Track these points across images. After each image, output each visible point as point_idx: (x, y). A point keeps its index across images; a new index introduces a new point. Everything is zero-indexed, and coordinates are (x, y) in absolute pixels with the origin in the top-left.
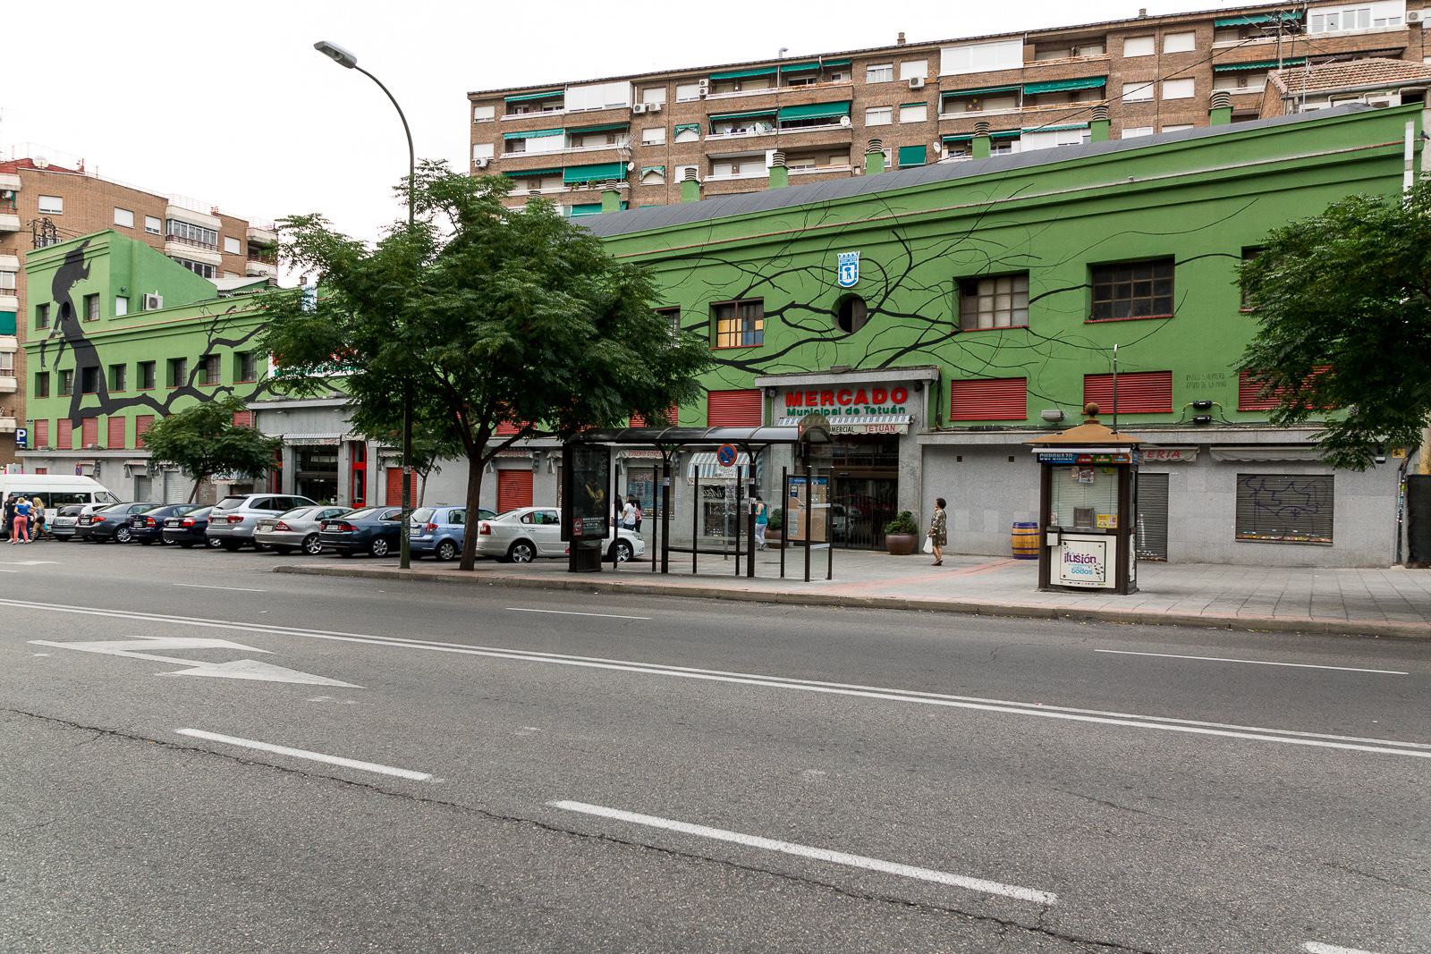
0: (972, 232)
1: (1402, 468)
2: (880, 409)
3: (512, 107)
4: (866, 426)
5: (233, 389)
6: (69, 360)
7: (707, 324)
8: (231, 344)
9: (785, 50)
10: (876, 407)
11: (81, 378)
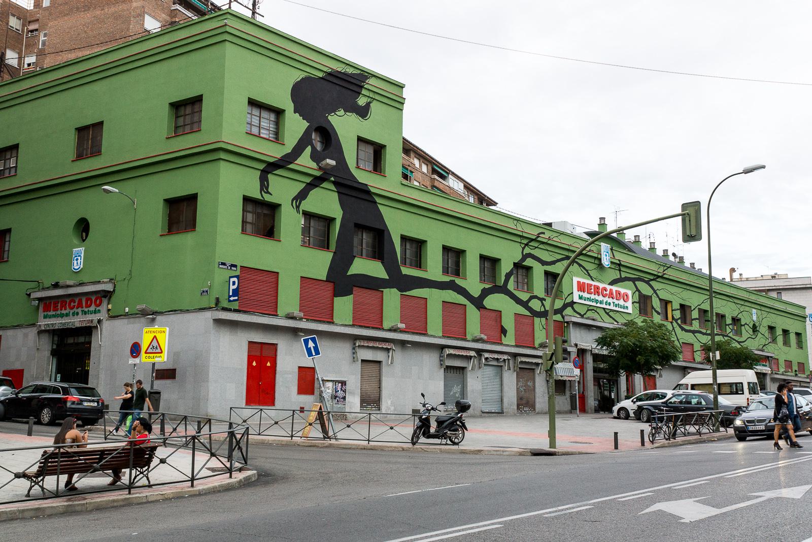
5: (545, 300)
8: (544, 263)
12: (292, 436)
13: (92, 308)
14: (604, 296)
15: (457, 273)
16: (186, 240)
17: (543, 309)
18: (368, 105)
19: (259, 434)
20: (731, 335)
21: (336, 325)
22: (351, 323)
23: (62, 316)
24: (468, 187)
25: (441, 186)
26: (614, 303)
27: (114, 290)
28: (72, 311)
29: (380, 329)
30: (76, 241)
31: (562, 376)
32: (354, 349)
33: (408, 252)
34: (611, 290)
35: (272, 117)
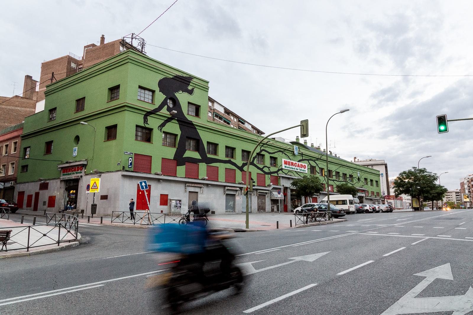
5: (270, 168)
8: (270, 153)
12: (134, 223)
13: (79, 171)
14: (296, 166)
15: (232, 157)
16: (112, 143)
17: (269, 171)
18: (193, 90)
19: (123, 223)
20: (349, 182)
21: (178, 177)
22: (184, 177)
23: (69, 174)
24: (253, 127)
25: (242, 126)
26: (299, 169)
27: (87, 164)
28: (72, 173)
29: (197, 179)
30: (75, 145)
31: (276, 198)
32: (185, 187)
33: (211, 148)
34: (298, 164)
35: (151, 93)
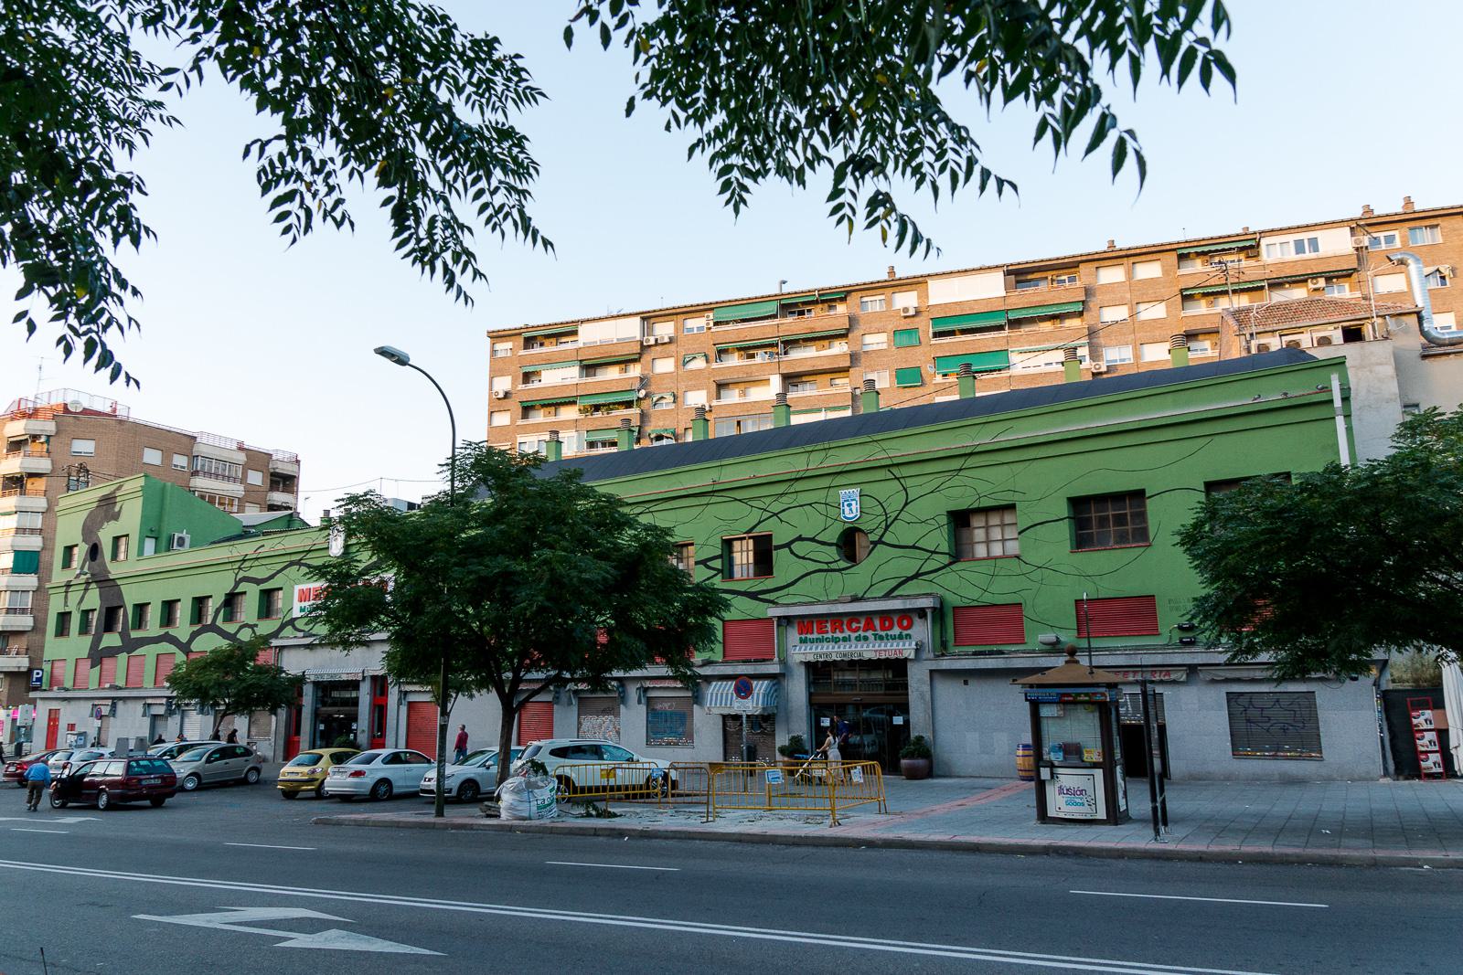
0: (960, 470)
1: (1376, 684)
2: (887, 635)
3: (529, 342)
4: (876, 651)
5: (256, 626)
6: (93, 599)
7: (721, 557)
8: (258, 581)
9: (784, 282)
10: (883, 633)
11: (103, 618)
